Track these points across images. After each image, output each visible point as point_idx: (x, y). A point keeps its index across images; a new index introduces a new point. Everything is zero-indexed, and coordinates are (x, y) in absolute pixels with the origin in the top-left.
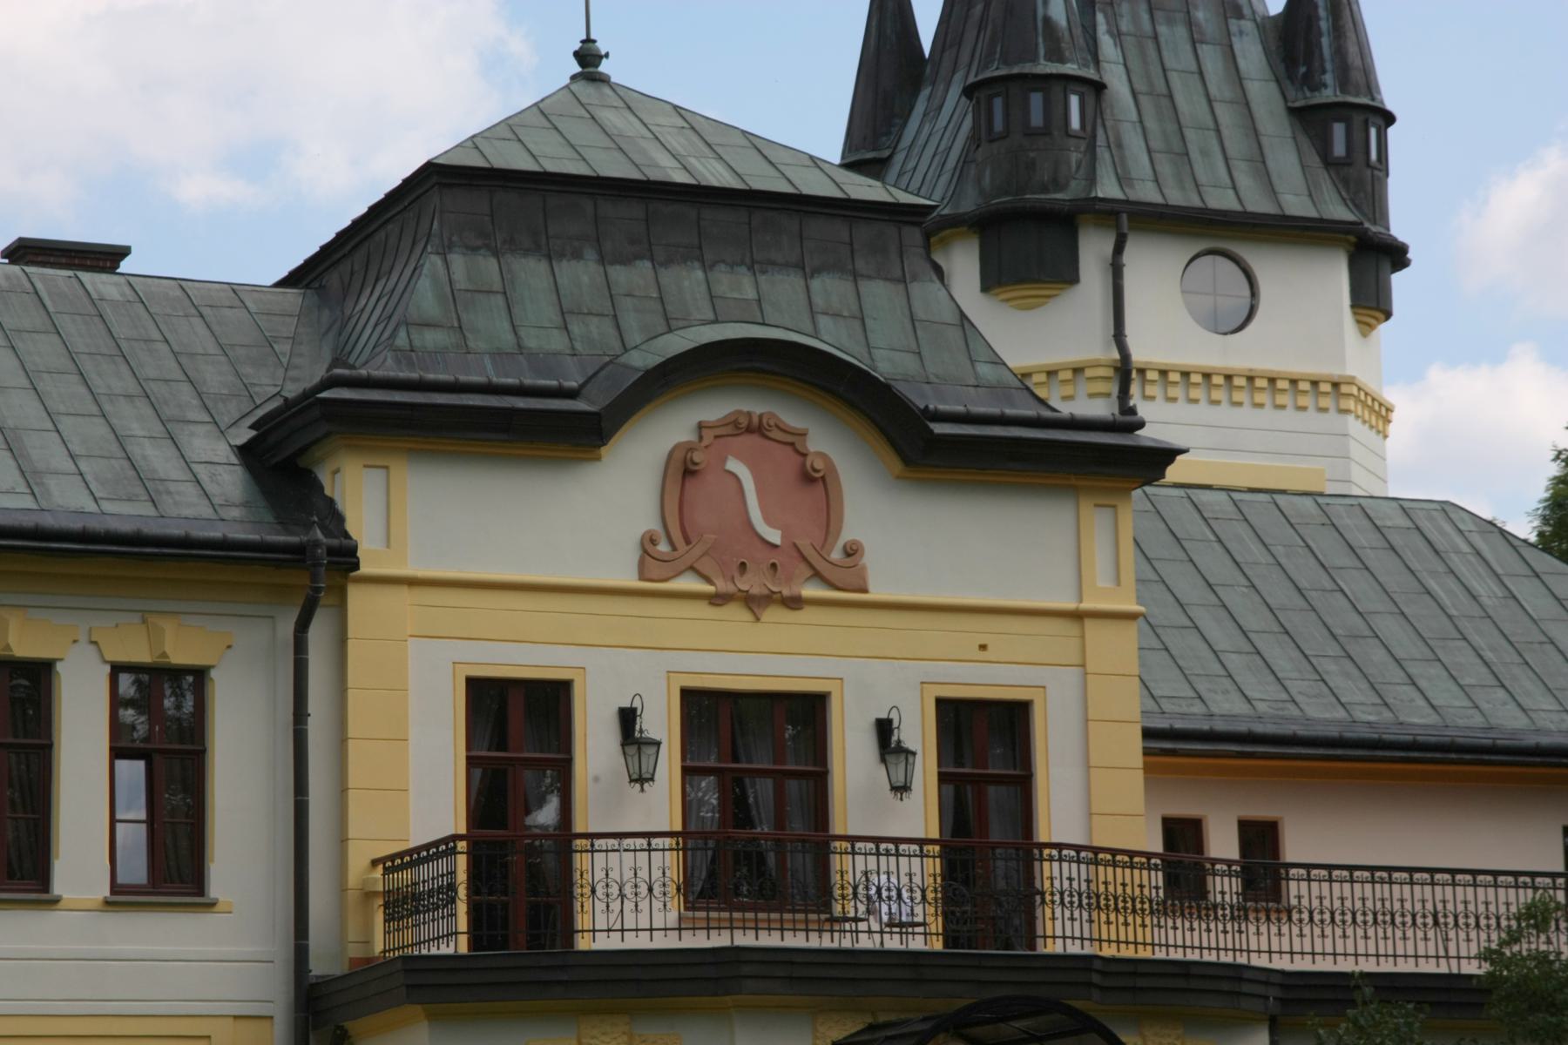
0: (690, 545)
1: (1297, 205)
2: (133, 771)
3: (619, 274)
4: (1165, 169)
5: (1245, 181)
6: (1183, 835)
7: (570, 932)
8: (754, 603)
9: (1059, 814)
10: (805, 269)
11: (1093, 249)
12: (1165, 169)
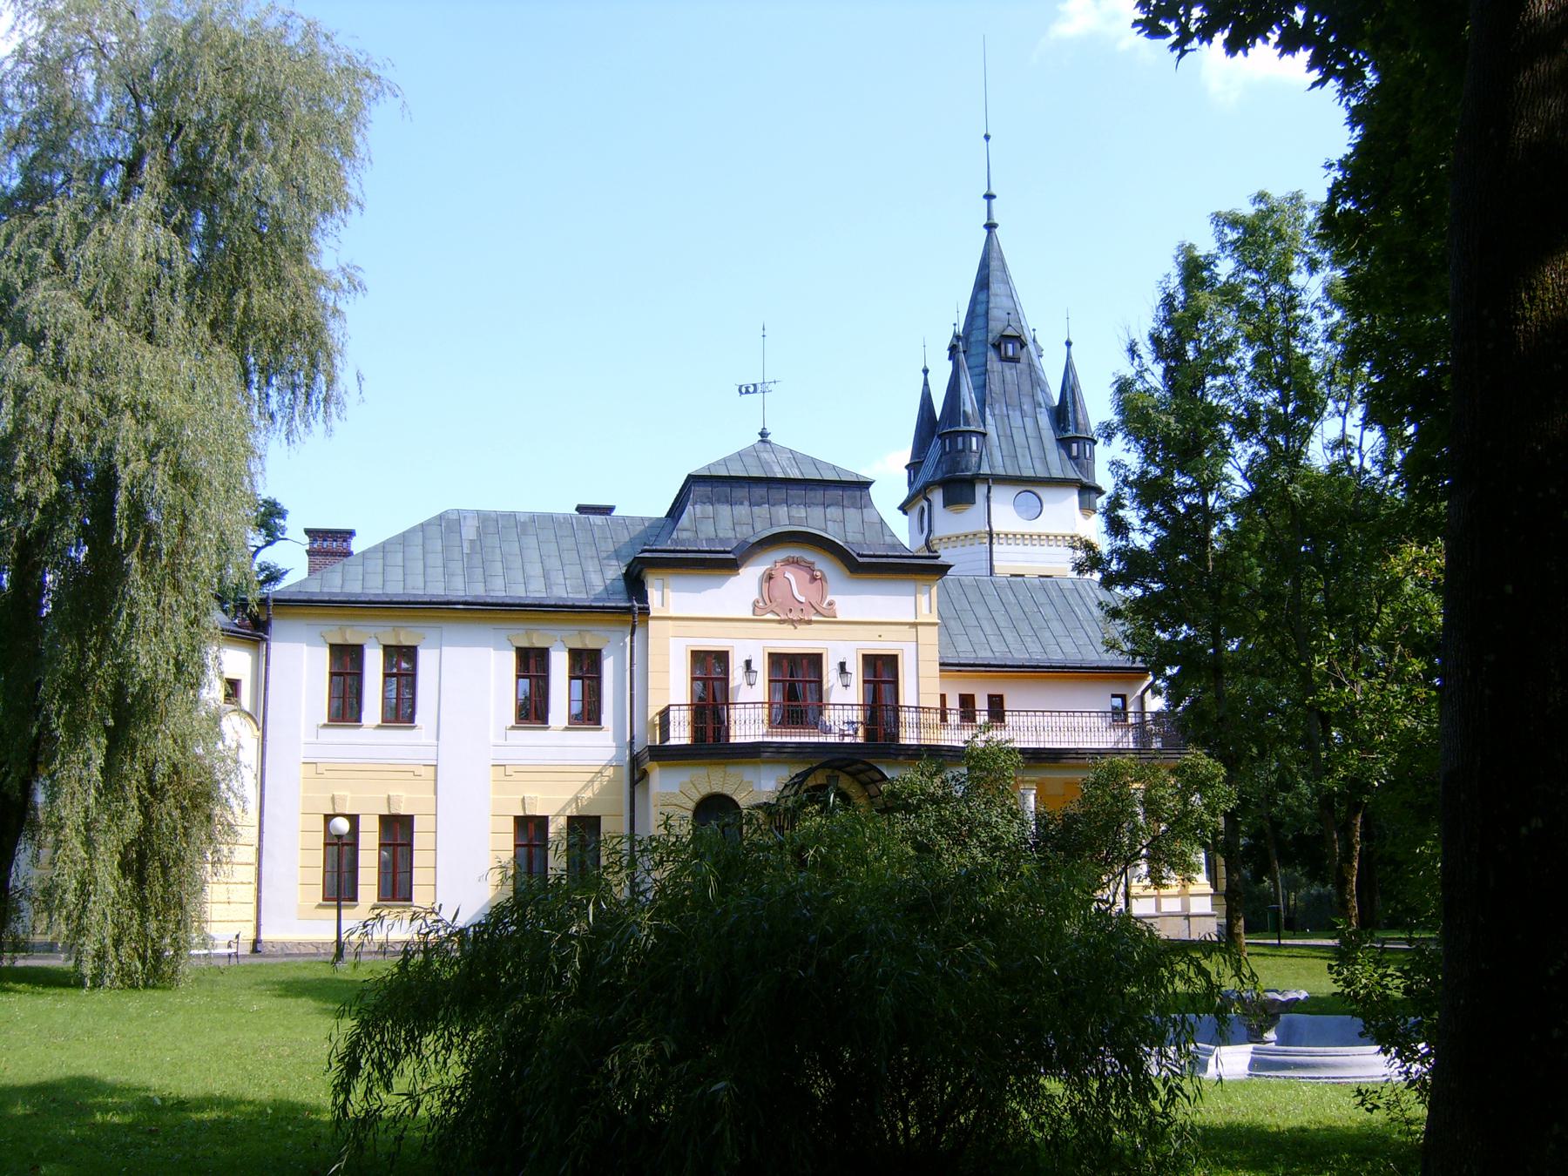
0: (770, 604)
1: (1056, 473)
2: (525, 683)
3: (756, 509)
4: (1008, 462)
5: (1038, 466)
6: (967, 701)
7: (728, 736)
8: (792, 622)
9: (907, 696)
10: (825, 506)
11: (980, 490)
12: (1008, 462)
